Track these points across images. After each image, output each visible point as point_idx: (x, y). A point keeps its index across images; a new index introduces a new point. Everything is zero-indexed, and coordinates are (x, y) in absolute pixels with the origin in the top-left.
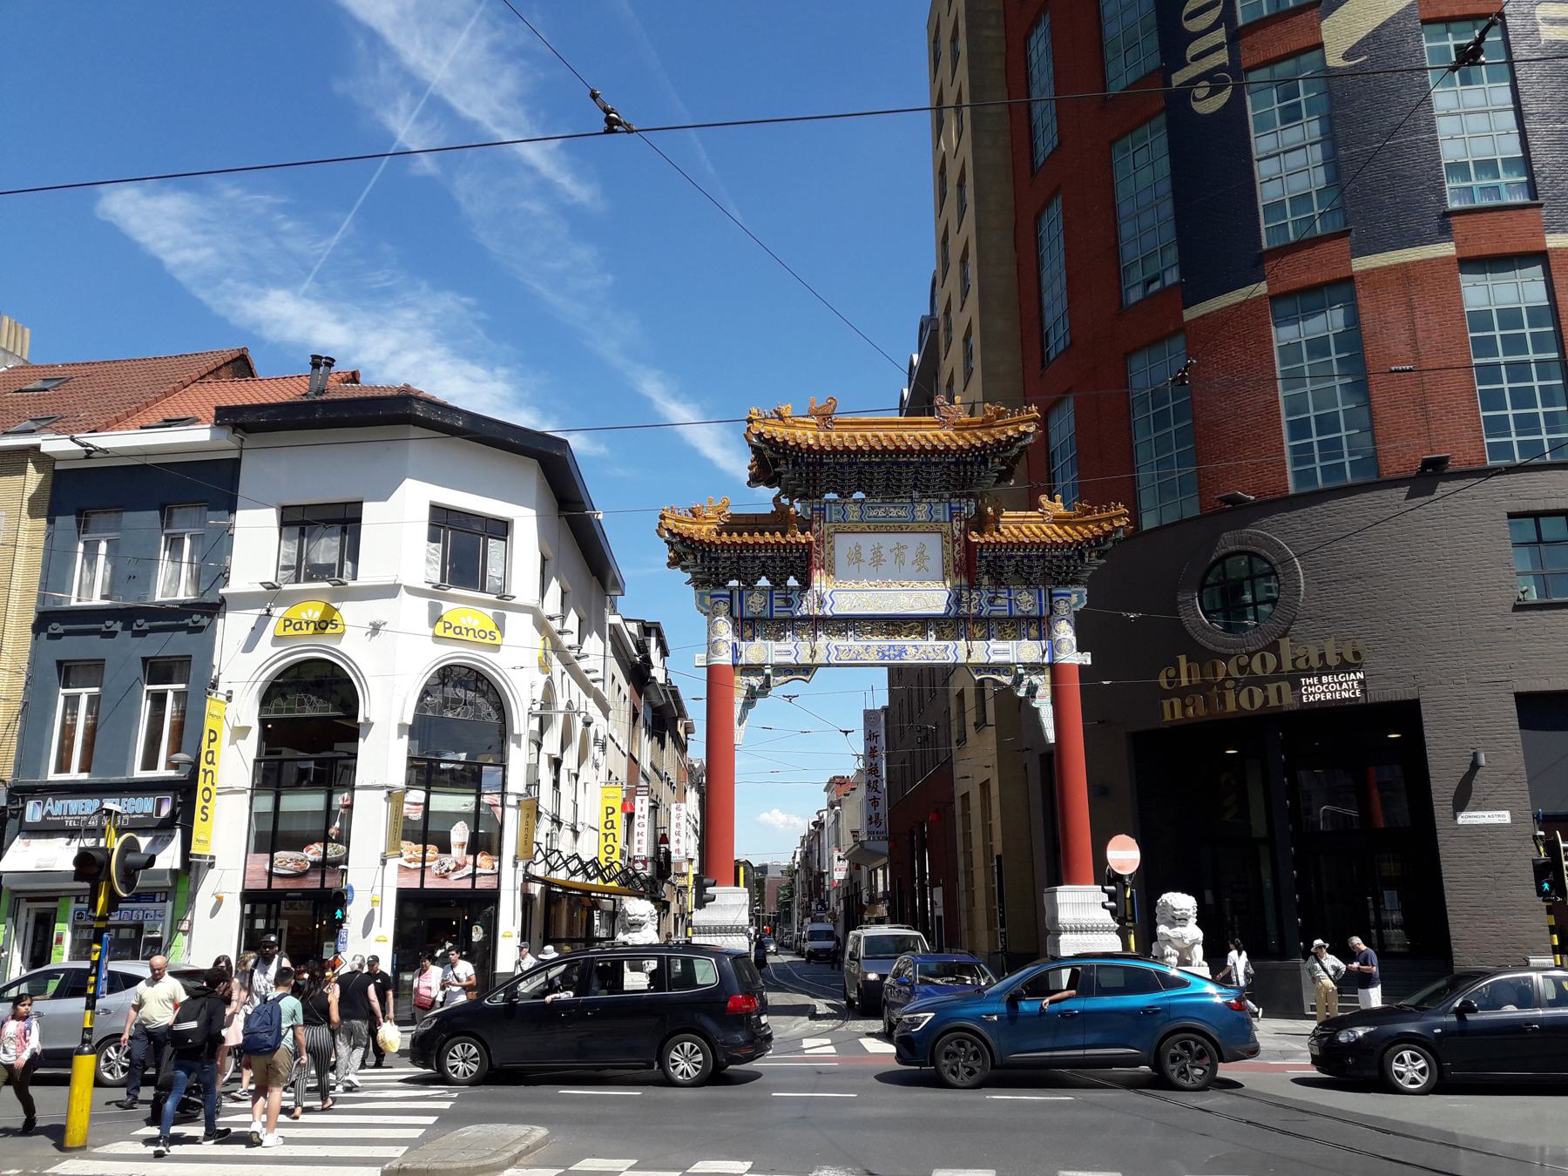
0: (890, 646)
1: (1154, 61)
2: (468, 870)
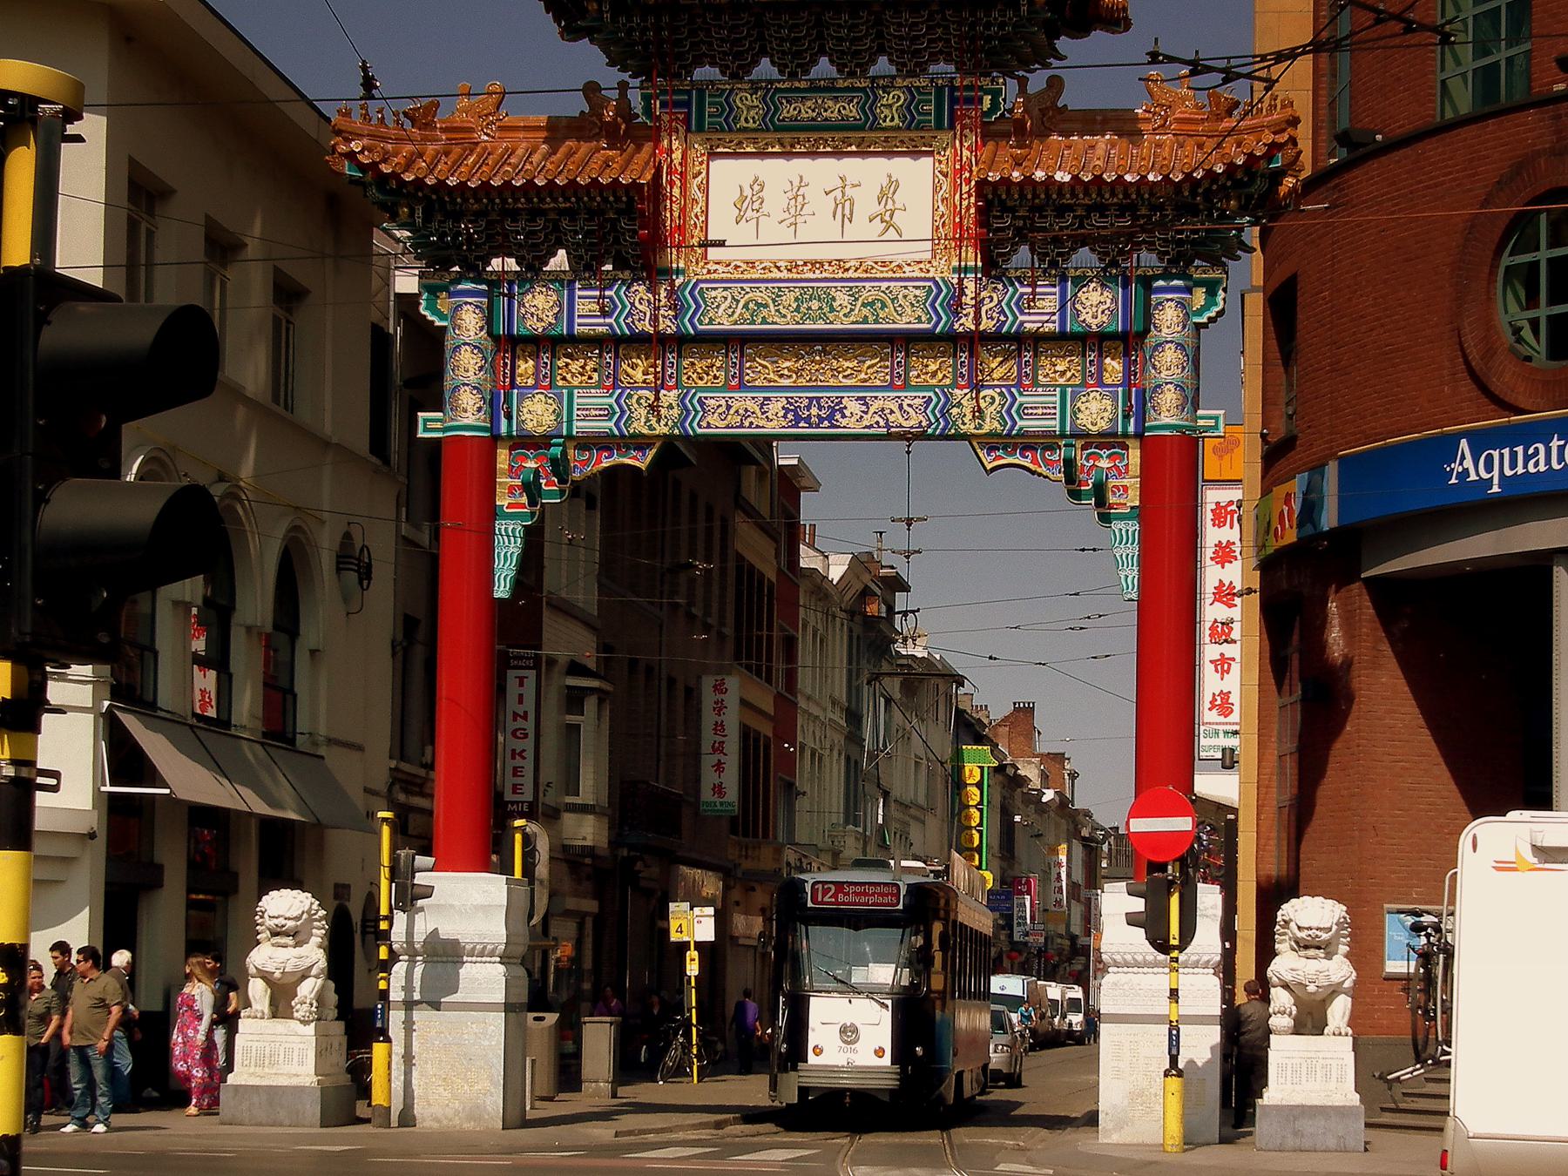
0: (811, 399)
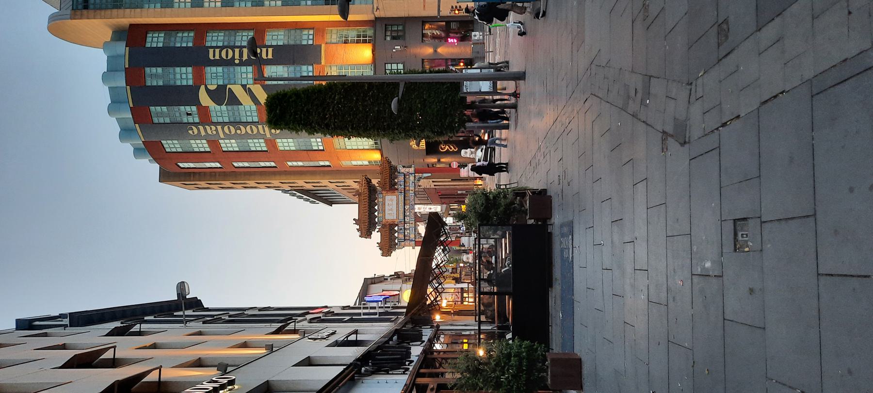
1: (262, 141)
2: (457, 294)
